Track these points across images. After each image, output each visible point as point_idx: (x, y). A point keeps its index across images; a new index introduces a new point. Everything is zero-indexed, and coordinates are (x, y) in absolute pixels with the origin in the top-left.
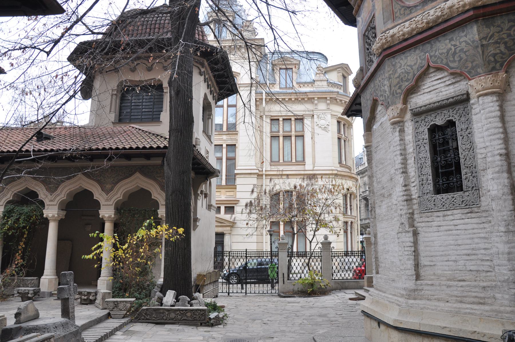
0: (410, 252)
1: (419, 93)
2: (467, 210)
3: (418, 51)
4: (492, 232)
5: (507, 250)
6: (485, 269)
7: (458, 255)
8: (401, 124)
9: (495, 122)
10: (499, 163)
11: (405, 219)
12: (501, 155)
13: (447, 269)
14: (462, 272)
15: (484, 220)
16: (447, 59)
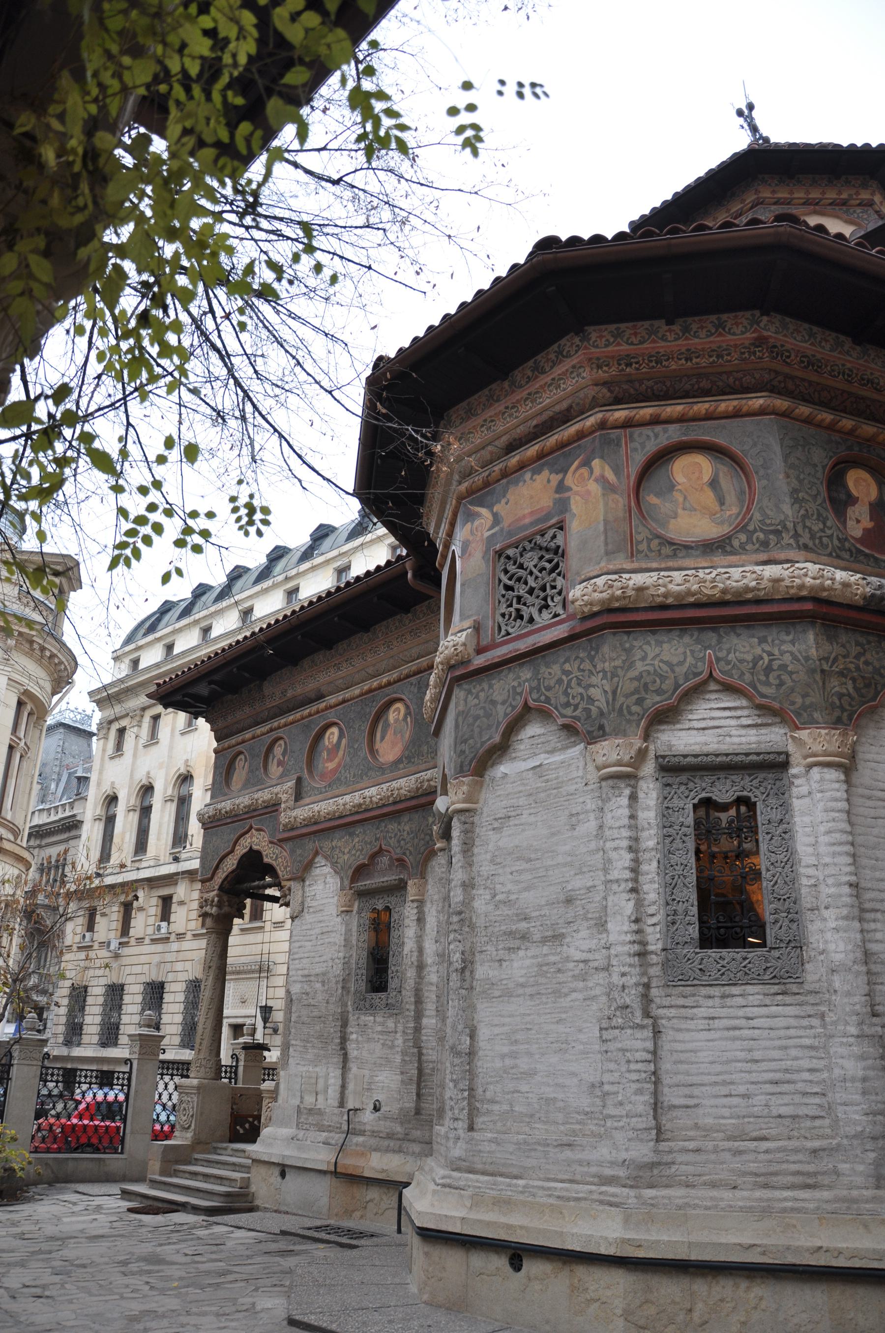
0: (644, 1075)
1: (678, 726)
2: (776, 987)
3: (687, 639)
4: (831, 1036)
5: (860, 1073)
6: (811, 1114)
7: (752, 1083)
8: (632, 782)
9: (842, 820)
10: (848, 900)
11: (632, 998)
12: (851, 885)
13: (727, 1114)
14: (761, 1120)
15: (810, 1010)
16: (752, 674)
